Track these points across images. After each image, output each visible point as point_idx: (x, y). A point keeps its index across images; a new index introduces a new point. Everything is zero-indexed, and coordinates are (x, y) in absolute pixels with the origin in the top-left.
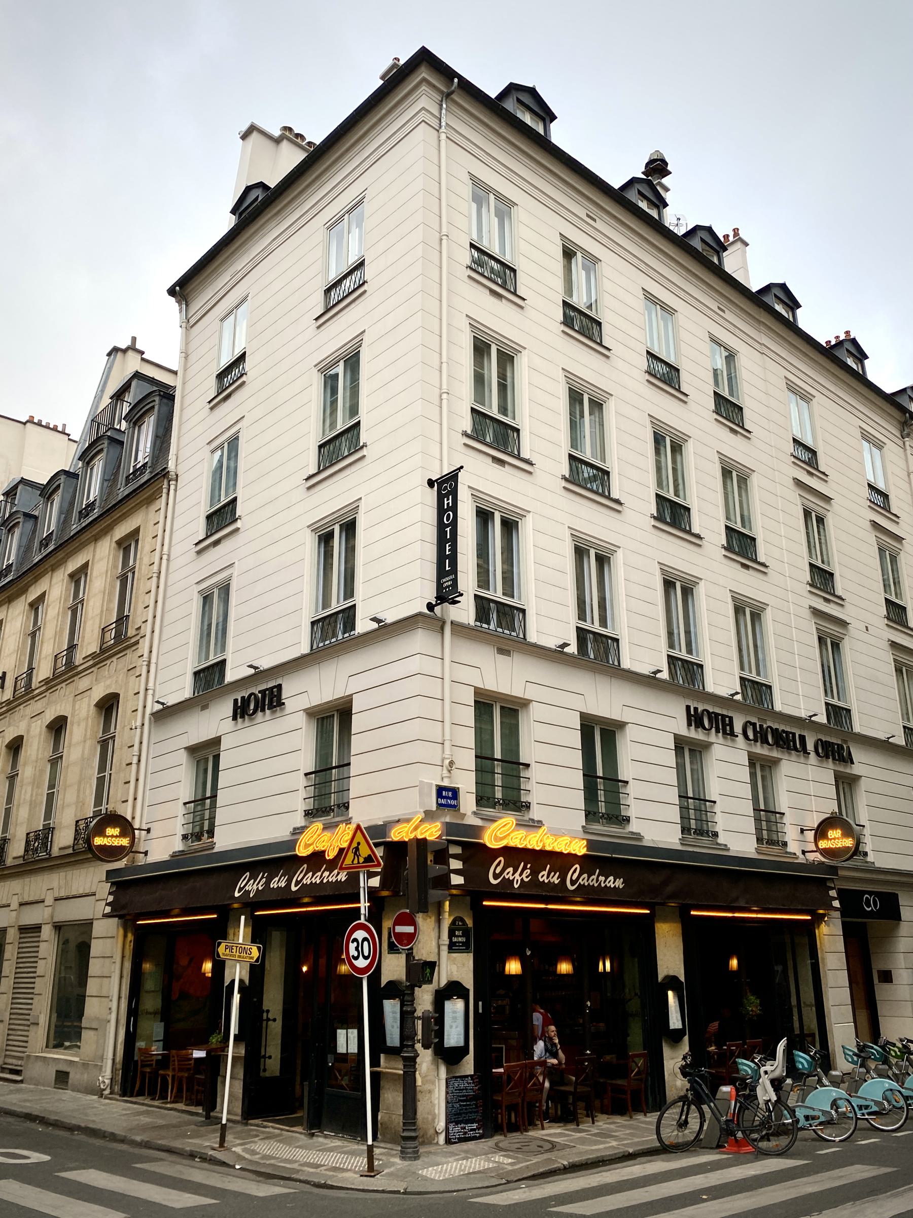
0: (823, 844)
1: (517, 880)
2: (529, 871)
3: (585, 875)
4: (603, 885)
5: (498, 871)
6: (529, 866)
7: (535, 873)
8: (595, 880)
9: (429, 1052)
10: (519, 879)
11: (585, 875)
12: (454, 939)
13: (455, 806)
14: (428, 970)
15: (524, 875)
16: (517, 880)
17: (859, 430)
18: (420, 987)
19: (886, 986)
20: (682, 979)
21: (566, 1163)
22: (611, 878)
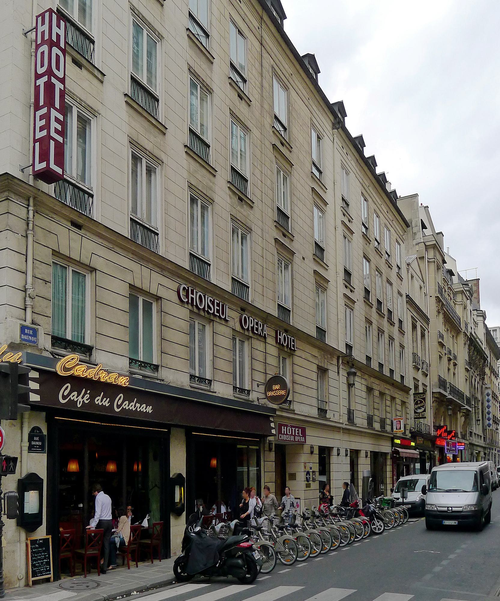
0: (270, 394)
1: (80, 402)
2: (88, 395)
3: (127, 402)
4: (138, 410)
5: (65, 394)
6: (89, 392)
7: (92, 398)
8: (133, 406)
9: (13, 522)
10: (82, 401)
11: (127, 402)
12: (33, 443)
13: (34, 342)
14: (11, 464)
15: (85, 399)
16: (80, 402)
17: (341, 161)
18: (6, 476)
19: (294, 482)
20: (185, 476)
21: (105, 596)
22: (144, 405)
